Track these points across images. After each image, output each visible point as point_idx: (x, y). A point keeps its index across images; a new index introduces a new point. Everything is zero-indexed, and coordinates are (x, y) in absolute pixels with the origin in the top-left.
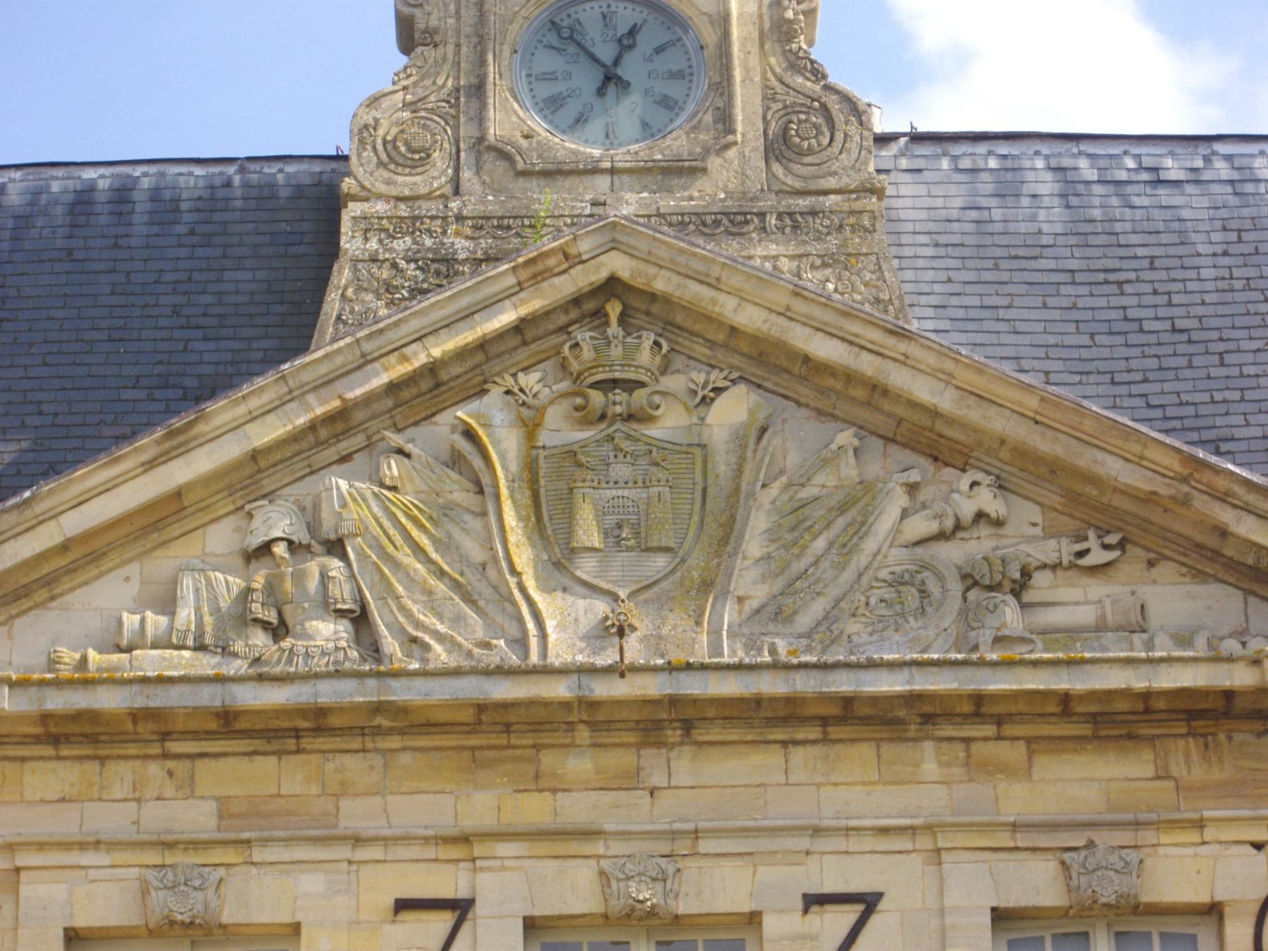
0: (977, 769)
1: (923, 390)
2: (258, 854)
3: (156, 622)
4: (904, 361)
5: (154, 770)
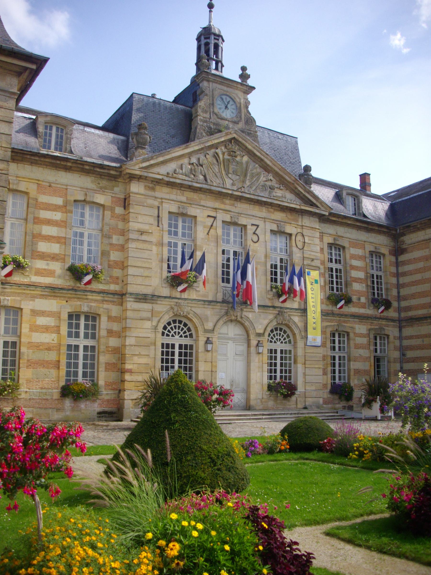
0: (269, 212)
1: (268, 162)
3: (181, 171)
4: (267, 158)
5: (179, 191)
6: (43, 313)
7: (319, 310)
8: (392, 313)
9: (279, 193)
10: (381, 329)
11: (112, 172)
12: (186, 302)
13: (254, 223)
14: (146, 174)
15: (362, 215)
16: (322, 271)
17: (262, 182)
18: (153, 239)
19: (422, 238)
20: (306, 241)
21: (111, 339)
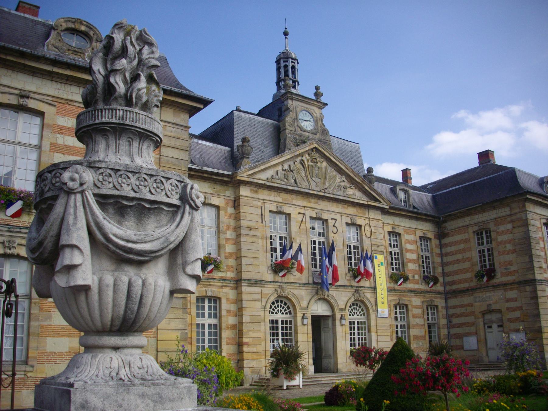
0: (344, 207)
2: (287, 205)
5: (276, 193)
7: (386, 288)
8: (439, 288)
9: (350, 192)
10: (431, 301)
11: (225, 179)
12: (287, 284)
13: (333, 218)
14: (252, 180)
15: (412, 207)
16: (385, 254)
17: (338, 183)
18: (259, 233)
19: (462, 224)
20: (373, 231)
21: (230, 317)
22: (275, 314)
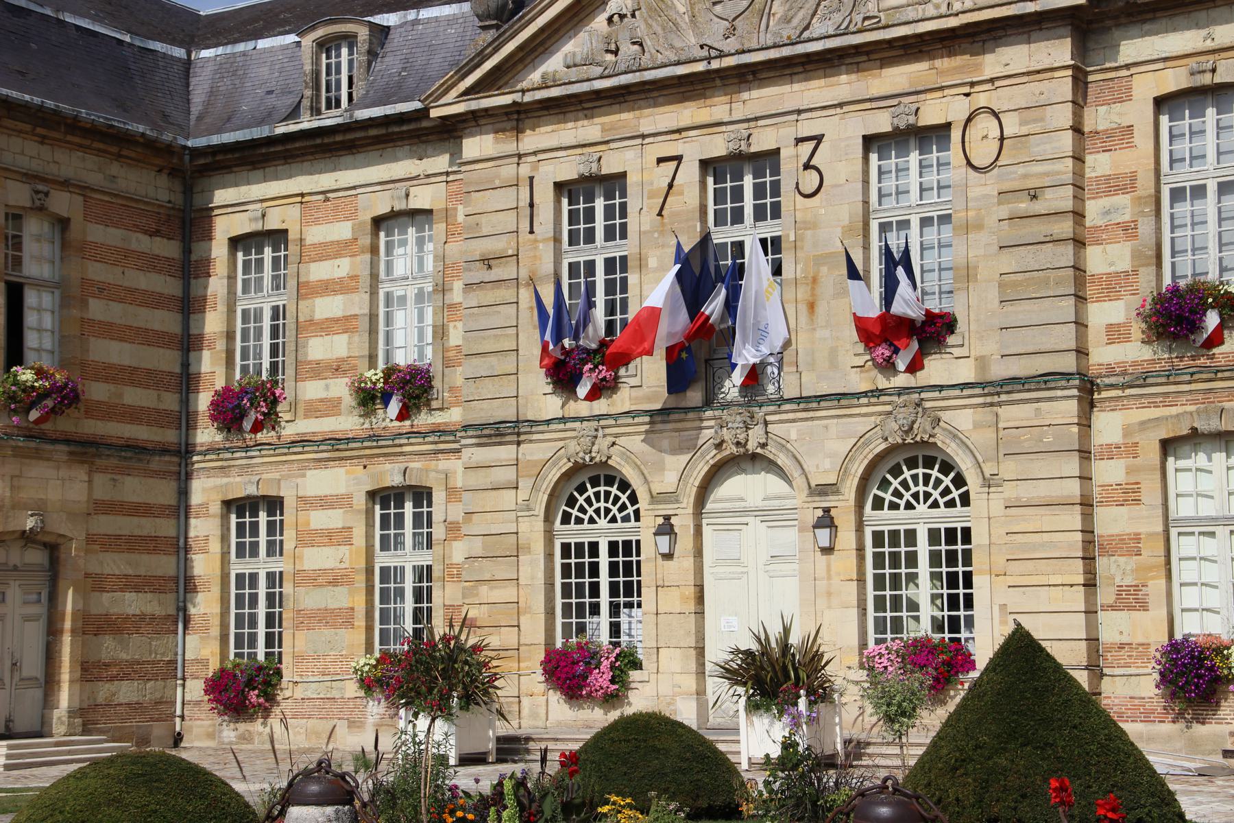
2: (612, 145)
6: (325, 502)
22: (586, 525)
